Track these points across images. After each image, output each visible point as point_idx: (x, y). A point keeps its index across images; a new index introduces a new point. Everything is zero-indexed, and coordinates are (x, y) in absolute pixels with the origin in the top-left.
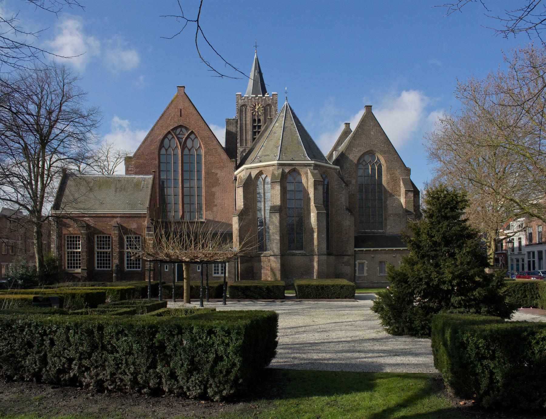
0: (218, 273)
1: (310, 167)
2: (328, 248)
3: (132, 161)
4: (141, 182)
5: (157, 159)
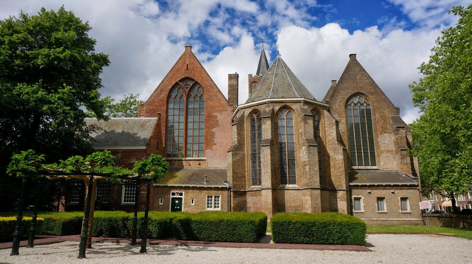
0: (211, 207)
1: (300, 104)
2: (321, 183)
4: (147, 123)
5: (165, 106)
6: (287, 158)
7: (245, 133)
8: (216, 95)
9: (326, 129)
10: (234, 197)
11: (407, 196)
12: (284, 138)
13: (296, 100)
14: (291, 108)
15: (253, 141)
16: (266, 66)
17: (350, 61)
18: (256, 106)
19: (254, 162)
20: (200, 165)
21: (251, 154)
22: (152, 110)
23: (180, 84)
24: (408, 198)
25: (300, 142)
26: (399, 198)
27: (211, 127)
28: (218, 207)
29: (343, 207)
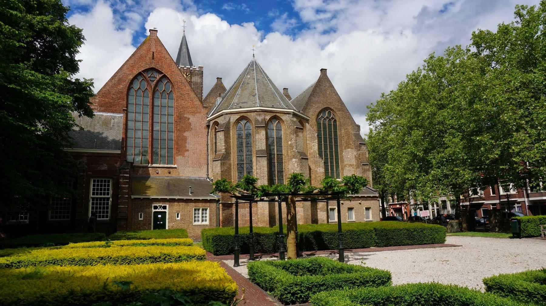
0: (198, 221)
1: (289, 115)
3: (95, 99)
4: (111, 120)
5: (125, 100)
6: (276, 170)
7: (231, 141)
8: (188, 94)
9: (308, 142)
10: (223, 210)
11: (370, 206)
12: (274, 149)
13: (286, 112)
14: (281, 119)
15: (240, 150)
16: (187, 56)
17: (321, 75)
18: (245, 112)
19: (241, 173)
20: (170, 173)
21: (237, 164)
22: (107, 103)
23: (144, 75)
24: (370, 208)
25: (289, 154)
26: (365, 208)
27: (182, 130)
28: (206, 220)
29: (323, 217)
